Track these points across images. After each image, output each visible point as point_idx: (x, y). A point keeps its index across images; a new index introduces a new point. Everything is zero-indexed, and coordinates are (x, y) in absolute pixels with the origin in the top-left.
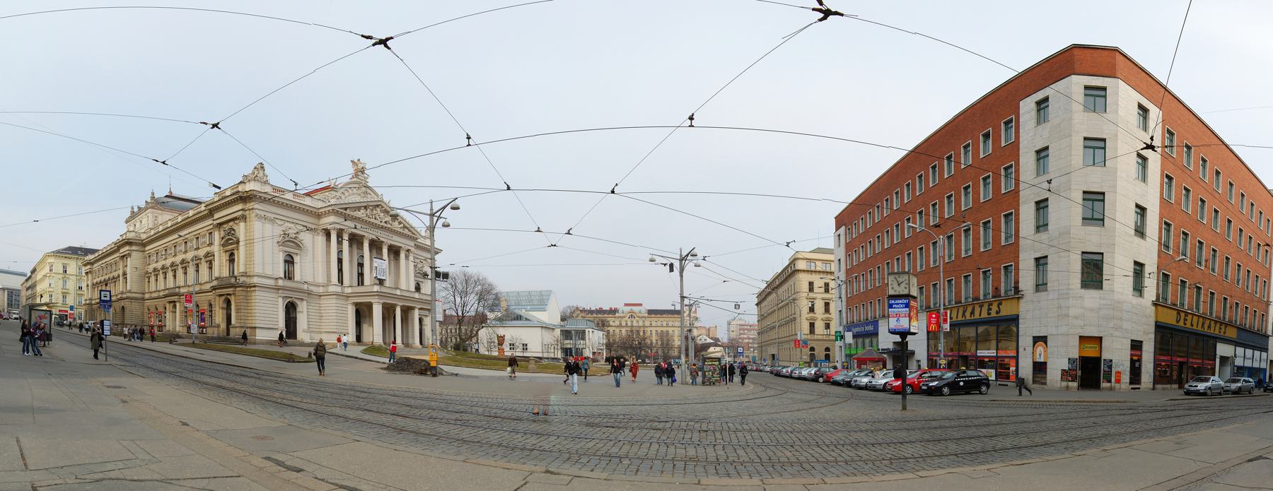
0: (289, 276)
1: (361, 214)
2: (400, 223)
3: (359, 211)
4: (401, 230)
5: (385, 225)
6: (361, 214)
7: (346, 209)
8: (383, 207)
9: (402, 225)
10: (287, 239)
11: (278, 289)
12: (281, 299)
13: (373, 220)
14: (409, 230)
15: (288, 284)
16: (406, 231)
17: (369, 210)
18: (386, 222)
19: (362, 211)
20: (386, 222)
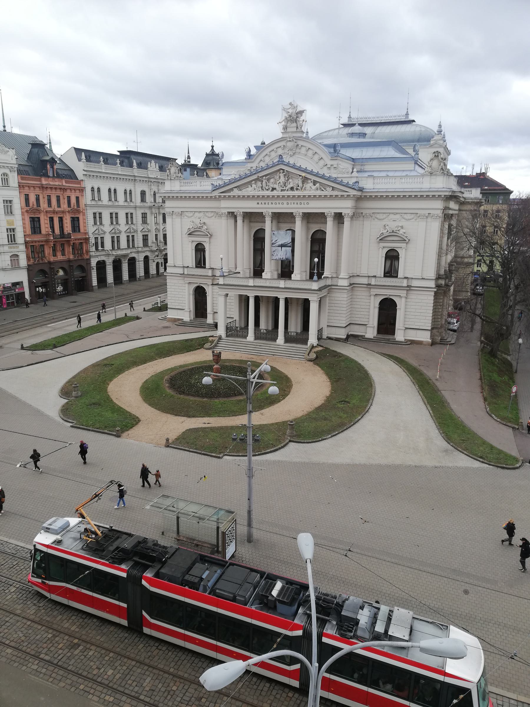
0: (200, 263)
2: (315, 183)
4: (319, 193)
5: (291, 193)
6: (249, 191)
7: (232, 190)
9: (318, 184)
10: (192, 230)
12: (187, 285)
14: (333, 189)
15: (200, 271)
16: (329, 192)
18: (292, 189)
19: (254, 186)
20: (292, 189)
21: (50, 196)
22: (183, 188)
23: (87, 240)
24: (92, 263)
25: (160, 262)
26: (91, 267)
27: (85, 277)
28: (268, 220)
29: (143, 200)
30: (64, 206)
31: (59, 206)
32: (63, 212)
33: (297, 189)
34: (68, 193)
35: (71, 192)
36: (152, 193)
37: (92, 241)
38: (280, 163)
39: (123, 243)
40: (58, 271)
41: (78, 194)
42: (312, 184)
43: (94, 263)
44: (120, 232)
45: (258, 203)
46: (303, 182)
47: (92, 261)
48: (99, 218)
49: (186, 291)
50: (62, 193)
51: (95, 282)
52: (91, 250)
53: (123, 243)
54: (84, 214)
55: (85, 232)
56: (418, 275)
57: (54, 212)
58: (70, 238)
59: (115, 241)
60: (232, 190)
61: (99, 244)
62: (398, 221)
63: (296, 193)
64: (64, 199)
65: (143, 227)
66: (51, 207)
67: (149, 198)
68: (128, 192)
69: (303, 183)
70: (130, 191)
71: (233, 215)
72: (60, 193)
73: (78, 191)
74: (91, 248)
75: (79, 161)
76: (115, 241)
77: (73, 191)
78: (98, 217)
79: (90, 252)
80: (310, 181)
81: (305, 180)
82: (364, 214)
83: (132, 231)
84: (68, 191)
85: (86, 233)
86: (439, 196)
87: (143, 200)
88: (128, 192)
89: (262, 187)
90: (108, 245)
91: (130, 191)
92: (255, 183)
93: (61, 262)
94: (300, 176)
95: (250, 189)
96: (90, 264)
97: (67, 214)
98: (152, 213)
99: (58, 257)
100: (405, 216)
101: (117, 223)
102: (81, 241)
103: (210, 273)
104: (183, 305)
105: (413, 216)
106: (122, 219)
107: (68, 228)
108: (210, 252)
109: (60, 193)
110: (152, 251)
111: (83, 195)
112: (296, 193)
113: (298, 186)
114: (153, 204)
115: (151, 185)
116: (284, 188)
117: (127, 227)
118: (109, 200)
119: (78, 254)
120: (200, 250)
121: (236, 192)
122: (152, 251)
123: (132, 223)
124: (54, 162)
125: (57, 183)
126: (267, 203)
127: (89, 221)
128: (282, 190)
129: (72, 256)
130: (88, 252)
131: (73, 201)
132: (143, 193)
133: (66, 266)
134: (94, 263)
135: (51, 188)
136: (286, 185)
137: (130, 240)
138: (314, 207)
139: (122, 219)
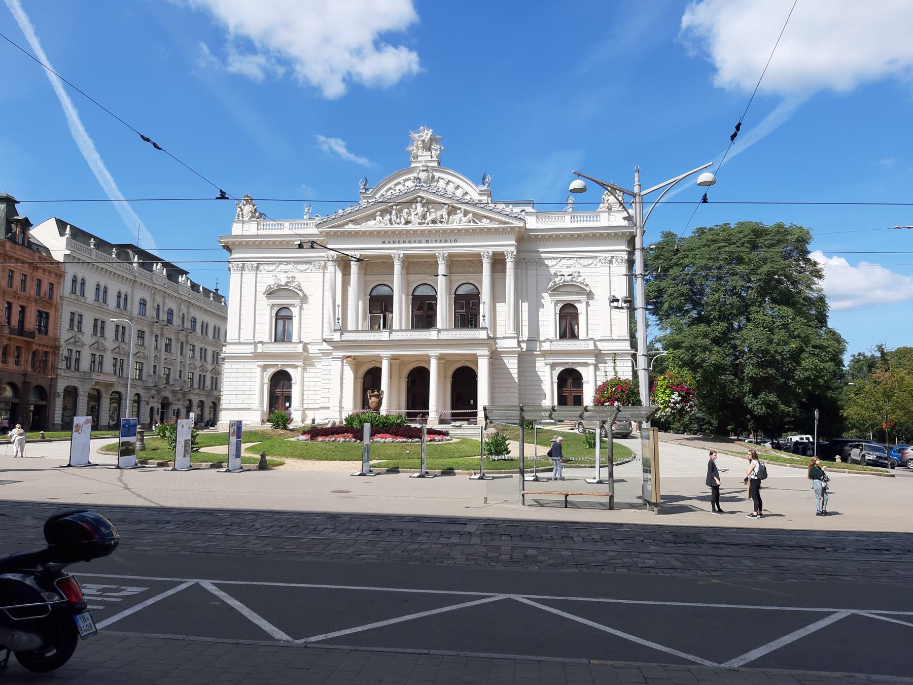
0: (282, 335)
1: (371, 225)
2: (466, 213)
3: (375, 220)
4: (472, 225)
5: (431, 226)
6: (371, 225)
8: (422, 198)
11: (257, 356)
13: (402, 227)
16: (485, 224)
17: (394, 212)
18: (434, 222)
19: (378, 218)
20: (434, 222)
21: (12, 271)
22: (261, 232)
23: (56, 348)
24: (58, 387)
25: (156, 407)
26: (55, 393)
27: (45, 406)
28: (397, 268)
29: (143, 313)
30: (31, 291)
31: (24, 289)
32: (28, 299)
33: (441, 222)
34: (39, 274)
35: (44, 274)
36: (156, 305)
37: (64, 352)
38: (417, 188)
39: (108, 366)
40: (4, 389)
41: (53, 279)
42: (462, 215)
43: (61, 387)
44: (105, 350)
45: (384, 242)
46: (449, 214)
47: (58, 384)
48: (78, 322)
49: (258, 379)
50: (31, 272)
51: (58, 419)
52: (59, 367)
53: (108, 366)
54: (57, 310)
55: (55, 337)
56: (606, 333)
57: (15, 295)
58: (34, 338)
59: (97, 363)
60: (347, 224)
61: (73, 362)
62: (572, 267)
63: (439, 226)
64: (33, 280)
65: (138, 351)
66: (11, 287)
67: (150, 311)
68: (123, 296)
69: (449, 216)
70: (126, 295)
71: (344, 263)
72: (28, 271)
73: (53, 275)
74: (60, 363)
75: (61, 236)
76: (97, 363)
77: (47, 273)
78: (76, 321)
79: (58, 368)
80: (459, 211)
81: (452, 211)
82: (526, 260)
83: (122, 352)
84: (40, 271)
85: (56, 339)
86: (623, 233)
87: (143, 313)
88: (123, 296)
89: (390, 221)
90: (85, 364)
91: (126, 295)
92: (382, 215)
93: (11, 373)
94: (445, 204)
95: (373, 222)
96: (56, 386)
97: (34, 304)
98: (152, 332)
99: (10, 365)
100: (581, 261)
101: (102, 336)
102: (47, 350)
103: (300, 348)
104: (250, 401)
105: (591, 261)
106: (110, 332)
107: (31, 322)
108: (300, 319)
109: (28, 271)
110: (147, 389)
111: (61, 283)
112: (439, 226)
113: (443, 218)
114: (156, 320)
115: (155, 294)
116: (424, 221)
117: (115, 346)
118: (96, 300)
119: (40, 367)
120: (282, 317)
121: (351, 227)
122: (147, 389)
123: (123, 341)
124: (27, 226)
125: (25, 254)
126: (397, 242)
127: (63, 320)
128: (419, 224)
129: (30, 368)
130: (55, 368)
131: (45, 287)
132: (143, 303)
133: (18, 382)
134: (61, 387)
135: (17, 259)
136: (426, 217)
137: (119, 366)
138: (463, 247)
139: (110, 332)
